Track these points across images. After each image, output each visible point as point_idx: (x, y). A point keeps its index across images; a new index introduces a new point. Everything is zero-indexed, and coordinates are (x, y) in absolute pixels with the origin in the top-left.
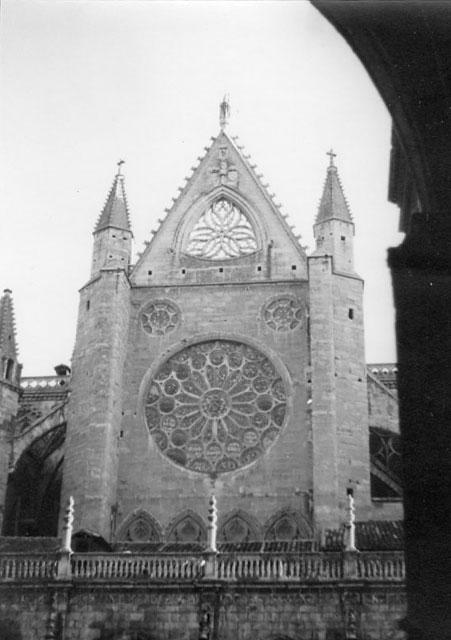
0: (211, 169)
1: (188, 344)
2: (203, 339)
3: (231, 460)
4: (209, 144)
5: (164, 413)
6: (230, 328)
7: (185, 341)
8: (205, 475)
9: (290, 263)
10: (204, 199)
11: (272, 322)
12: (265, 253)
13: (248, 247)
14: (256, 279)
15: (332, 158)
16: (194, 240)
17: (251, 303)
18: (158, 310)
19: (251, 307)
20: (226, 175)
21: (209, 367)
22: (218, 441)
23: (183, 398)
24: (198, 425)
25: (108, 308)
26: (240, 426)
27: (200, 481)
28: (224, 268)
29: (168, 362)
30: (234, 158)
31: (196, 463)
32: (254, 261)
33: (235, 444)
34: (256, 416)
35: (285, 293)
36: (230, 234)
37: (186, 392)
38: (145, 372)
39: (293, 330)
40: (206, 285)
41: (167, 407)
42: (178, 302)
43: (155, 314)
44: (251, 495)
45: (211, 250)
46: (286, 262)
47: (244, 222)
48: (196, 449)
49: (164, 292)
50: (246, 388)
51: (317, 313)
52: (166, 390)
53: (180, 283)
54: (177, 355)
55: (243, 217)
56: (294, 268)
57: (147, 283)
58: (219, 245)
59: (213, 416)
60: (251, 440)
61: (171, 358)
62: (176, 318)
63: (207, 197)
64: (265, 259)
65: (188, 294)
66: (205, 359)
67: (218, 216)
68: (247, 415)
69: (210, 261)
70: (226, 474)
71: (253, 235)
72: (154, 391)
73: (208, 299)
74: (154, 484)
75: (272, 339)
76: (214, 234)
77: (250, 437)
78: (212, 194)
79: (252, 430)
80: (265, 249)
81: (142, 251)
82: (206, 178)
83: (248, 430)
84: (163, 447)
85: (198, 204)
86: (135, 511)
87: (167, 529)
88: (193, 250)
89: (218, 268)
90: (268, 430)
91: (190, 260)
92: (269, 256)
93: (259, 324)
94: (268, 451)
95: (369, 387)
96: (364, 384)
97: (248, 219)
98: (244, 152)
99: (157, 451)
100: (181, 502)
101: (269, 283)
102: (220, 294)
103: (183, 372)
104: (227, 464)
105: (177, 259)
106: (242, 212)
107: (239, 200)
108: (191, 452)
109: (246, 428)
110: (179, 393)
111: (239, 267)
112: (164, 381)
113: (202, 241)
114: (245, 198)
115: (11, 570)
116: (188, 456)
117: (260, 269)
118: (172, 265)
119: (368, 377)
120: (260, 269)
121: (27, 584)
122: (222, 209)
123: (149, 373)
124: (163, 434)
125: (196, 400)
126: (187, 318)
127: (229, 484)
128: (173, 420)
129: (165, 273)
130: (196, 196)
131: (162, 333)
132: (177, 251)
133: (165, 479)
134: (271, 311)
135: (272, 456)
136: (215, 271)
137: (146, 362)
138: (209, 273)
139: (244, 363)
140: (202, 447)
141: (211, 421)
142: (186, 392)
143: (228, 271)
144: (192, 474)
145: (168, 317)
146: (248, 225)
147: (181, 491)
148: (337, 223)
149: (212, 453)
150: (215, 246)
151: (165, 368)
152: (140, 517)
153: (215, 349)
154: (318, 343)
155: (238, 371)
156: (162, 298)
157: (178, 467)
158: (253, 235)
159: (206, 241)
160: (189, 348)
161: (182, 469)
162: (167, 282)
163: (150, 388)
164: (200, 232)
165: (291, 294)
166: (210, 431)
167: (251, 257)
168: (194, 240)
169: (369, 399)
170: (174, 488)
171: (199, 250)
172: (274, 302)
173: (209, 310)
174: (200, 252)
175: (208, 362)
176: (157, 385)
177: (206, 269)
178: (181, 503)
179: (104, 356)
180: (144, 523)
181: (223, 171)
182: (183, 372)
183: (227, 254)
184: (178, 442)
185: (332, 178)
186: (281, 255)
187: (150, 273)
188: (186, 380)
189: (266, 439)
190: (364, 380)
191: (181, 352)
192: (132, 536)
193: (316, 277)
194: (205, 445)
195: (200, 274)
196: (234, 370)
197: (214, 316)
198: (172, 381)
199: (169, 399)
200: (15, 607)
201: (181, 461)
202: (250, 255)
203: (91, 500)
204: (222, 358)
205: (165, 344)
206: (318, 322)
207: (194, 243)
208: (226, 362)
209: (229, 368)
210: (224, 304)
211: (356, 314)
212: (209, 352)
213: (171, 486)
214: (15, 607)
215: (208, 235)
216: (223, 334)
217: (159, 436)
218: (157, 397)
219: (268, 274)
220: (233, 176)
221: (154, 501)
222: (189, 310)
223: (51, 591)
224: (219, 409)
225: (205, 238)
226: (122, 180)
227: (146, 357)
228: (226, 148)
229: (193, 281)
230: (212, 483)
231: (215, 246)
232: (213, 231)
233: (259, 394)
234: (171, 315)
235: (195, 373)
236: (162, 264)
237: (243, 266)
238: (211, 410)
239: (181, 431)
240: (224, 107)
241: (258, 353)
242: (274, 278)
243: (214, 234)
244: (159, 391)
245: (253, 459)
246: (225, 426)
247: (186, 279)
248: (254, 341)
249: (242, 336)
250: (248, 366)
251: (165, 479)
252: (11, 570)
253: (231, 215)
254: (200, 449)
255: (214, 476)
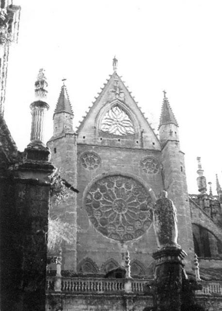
0: (111, 90)
1: (105, 176)
2: (113, 174)
3: (130, 234)
4: (109, 78)
5: (95, 209)
6: (125, 170)
7: (104, 174)
8: (118, 241)
9: (151, 141)
10: (109, 105)
11: (145, 170)
12: (140, 135)
13: (131, 131)
14: (136, 147)
15: (165, 94)
16: (104, 124)
17: (135, 159)
18: (89, 157)
19: (135, 161)
20: (119, 95)
21: (115, 188)
22: (123, 225)
23: (104, 202)
24: (112, 216)
25: (70, 153)
26: (132, 218)
27: (116, 244)
28: (121, 139)
29: (96, 183)
30: (122, 87)
31: (113, 235)
32: (135, 138)
33: (131, 227)
34: (140, 214)
35: (150, 156)
36: (121, 123)
37: (105, 199)
38: (85, 187)
39: (156, 174)
40: (112, 147)
41: (97, 205)
42: (99, 154)
43: (88, 159)
44: (141, 253)
45: (112, 130)
46: (151, 140)
47: (127, 118)
48: (112, 228)
49: (92, 148)
50: (134, 199)
51: (174, 167)
52: (95, 197)
53: (100, 144)
54: (100, 180)
55: (126, 115)
56: (154, 144)
57: (83, 142)
58: (116, 128)
59: (119, 212)
60: (138, 225)
61: (97, 182)
62: (99, 162)
63: (110, 104)
64: (140, 138)
65: (103, 151)
66: (114, 184)
67: (115, 114)
68: (136, 213)
69: (112, 135)
70: (128, 241)
71: (132, 125)
72: (89, 197)
73: (114, 154)
74: (93, 245)
75: (147, 177)
76: (114, 122)
77: (137, 224)
78: (112, 102)
79: (138, 220)
80: (140, 133)
81: (78, 126)
82: (109, 95)
83: (137, 221)
84: (96, 225)
85: (106, 106)
86: (85, 258)
87: (102, 267)
88: (104, 128)
89: (117, 139)
90: (146, 221)
91: (105, 134)
92: (142, 137)
93: (139, 169)
94: (147, 231)
95: (190, 204)
96: (188, 202)
97: (130, 118)
98: (126, 85)
99: (94, 227)
100: (107, 254)
101: (142, 150)
102: (119, 152)
103: (103, 189)
104: (130, 237)
105: (97, 132)
106: (127, 114)
107: (126, 107)
108: (110, 229)
109: (136, 219)
110: (101, 199)
111: (128, 140)
112: (94, 193)
113: (109, 125)
114: (128, 107)
115: (100, 287)
116: (109, 231)
117: (137, 142)
118: (95, 134)
119: (190, 200)
120: (137, 142)
121: (112, 294)
122: (117, 111)
123: (86, 189)
124: (95, 219)
125: (111, 203)
126: (104, 162)
127: (131, 247)
128: (99, 212)
129: (92, 138)
130: (105, 103)
131: (92, 168)
132: (97, 128)
133: (98, 242)
134: (145, 164)
135: (149, 234)
136: (116, 140)
137: (86, 182)
138: (113, 141)
139: (132, 188)
140: (115, 227)
141: (119, 215)
142: (105, 199)
143: (123, 141)
144: (112, 240)
145: (95, 161)
146: (129, 120)
147: (107, 249)
148: (173, 125)
149: (120, 231)
150: (114, 128)
151: (95, 186)
152: (87, 261)
153: (118, 179)
154: (176, 182)
155: (130, 192)
156: (91, 151)
157: (104, 236)
158: (132, 125)
159: (110, 125)
160: (106, 178)
161: (107, 238)
162: (93, 143)
163: (87, 195)
164: (107, 120)
165: (153, 156)
166: (118, 219)
167: (134, 136)
168: (104, 124)
169: (191, 210)
170: (104, 247)
171: (107, 129)
172: (145, 159)
173: (115, 159)
174: (107, 130)
175: (115, 186)
176: (90, 194)
177: (112, 139)
178: (107, 255)
179: (71, 178)
180: (89, 264)
181: (118, 92)
182: (103, 189)
183: (121, 133)
184: (103, 224)
185: (166, 105)
186: (147, 137)
187: (84, 137)
188: (105, 193)
189: (145, 225)
190: (188, 200)
191: (102, 179)
192: (83, 270)
193: (172, 150)
194: (117, 226)
195: (110, 142)
196: (128, 190)
197: (117, 163)
198: (98, 193)
199: (96, 202)
200: (106, 307)
201: (106, 234)
202: (133, 135)
203: (69, 251)
204: (121, 184)
205: (94, 175)
206: (175, 171)
207: (104, 125)
208: (123, 186)
209: (126, 189)
210: (122, 158)
211: (183, 168)
212: (115, 181)
213: (102, 246)
214: (106, 307)
215: (111, 122)
216: (123, 172)
217: (93, 220)
218: (91, 201)
219: (142, 145)
220: (122, 95)
221: (94, 253)
222: (105, 159)
223: (124, 299)
224: (121, 208)
225: (109, 123)
226: (65, 89)
227: (85, 180)
228: (118, 81)
229: (106, 144)
230: (122, 245)
231: (114, 128)
232: (113, 120)
233: (141, 203)
234: (96, 160)
235: (109, 190)
236: (90, 134)
237: (130, 140)
238: (118, 209)
239: (104, 219)
240: (115, 60)
241: (138, 183)
242: (145, 148)
243: (114, 122)
244: (92, 197)
245: (140, 235)
246: (125, 217)
247: (102, 143)
248: (139, 177)
249: (130, 173)
250: (134, 189)
251: (98, 242)
252: (100, 287)
253: (121, 114)
254: (114, 228)
255: (122, 242)
